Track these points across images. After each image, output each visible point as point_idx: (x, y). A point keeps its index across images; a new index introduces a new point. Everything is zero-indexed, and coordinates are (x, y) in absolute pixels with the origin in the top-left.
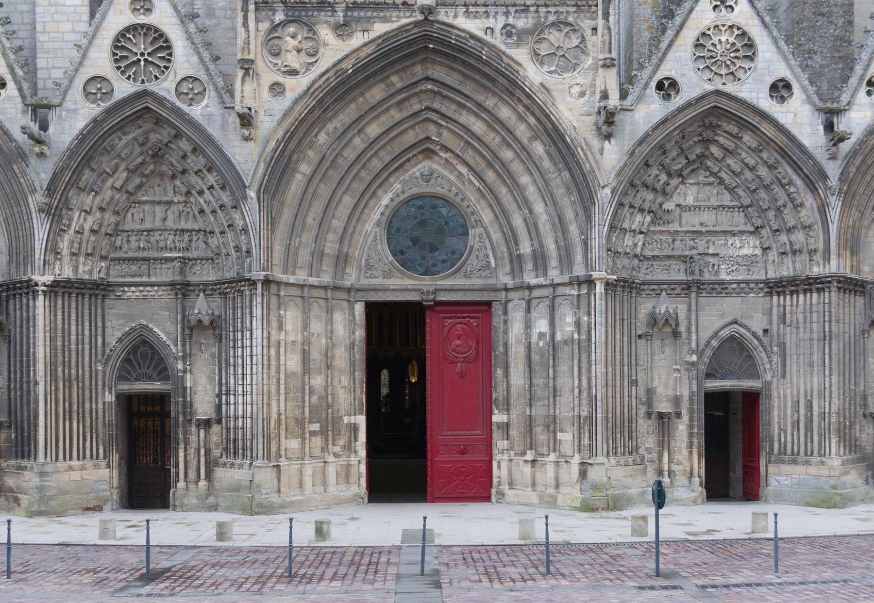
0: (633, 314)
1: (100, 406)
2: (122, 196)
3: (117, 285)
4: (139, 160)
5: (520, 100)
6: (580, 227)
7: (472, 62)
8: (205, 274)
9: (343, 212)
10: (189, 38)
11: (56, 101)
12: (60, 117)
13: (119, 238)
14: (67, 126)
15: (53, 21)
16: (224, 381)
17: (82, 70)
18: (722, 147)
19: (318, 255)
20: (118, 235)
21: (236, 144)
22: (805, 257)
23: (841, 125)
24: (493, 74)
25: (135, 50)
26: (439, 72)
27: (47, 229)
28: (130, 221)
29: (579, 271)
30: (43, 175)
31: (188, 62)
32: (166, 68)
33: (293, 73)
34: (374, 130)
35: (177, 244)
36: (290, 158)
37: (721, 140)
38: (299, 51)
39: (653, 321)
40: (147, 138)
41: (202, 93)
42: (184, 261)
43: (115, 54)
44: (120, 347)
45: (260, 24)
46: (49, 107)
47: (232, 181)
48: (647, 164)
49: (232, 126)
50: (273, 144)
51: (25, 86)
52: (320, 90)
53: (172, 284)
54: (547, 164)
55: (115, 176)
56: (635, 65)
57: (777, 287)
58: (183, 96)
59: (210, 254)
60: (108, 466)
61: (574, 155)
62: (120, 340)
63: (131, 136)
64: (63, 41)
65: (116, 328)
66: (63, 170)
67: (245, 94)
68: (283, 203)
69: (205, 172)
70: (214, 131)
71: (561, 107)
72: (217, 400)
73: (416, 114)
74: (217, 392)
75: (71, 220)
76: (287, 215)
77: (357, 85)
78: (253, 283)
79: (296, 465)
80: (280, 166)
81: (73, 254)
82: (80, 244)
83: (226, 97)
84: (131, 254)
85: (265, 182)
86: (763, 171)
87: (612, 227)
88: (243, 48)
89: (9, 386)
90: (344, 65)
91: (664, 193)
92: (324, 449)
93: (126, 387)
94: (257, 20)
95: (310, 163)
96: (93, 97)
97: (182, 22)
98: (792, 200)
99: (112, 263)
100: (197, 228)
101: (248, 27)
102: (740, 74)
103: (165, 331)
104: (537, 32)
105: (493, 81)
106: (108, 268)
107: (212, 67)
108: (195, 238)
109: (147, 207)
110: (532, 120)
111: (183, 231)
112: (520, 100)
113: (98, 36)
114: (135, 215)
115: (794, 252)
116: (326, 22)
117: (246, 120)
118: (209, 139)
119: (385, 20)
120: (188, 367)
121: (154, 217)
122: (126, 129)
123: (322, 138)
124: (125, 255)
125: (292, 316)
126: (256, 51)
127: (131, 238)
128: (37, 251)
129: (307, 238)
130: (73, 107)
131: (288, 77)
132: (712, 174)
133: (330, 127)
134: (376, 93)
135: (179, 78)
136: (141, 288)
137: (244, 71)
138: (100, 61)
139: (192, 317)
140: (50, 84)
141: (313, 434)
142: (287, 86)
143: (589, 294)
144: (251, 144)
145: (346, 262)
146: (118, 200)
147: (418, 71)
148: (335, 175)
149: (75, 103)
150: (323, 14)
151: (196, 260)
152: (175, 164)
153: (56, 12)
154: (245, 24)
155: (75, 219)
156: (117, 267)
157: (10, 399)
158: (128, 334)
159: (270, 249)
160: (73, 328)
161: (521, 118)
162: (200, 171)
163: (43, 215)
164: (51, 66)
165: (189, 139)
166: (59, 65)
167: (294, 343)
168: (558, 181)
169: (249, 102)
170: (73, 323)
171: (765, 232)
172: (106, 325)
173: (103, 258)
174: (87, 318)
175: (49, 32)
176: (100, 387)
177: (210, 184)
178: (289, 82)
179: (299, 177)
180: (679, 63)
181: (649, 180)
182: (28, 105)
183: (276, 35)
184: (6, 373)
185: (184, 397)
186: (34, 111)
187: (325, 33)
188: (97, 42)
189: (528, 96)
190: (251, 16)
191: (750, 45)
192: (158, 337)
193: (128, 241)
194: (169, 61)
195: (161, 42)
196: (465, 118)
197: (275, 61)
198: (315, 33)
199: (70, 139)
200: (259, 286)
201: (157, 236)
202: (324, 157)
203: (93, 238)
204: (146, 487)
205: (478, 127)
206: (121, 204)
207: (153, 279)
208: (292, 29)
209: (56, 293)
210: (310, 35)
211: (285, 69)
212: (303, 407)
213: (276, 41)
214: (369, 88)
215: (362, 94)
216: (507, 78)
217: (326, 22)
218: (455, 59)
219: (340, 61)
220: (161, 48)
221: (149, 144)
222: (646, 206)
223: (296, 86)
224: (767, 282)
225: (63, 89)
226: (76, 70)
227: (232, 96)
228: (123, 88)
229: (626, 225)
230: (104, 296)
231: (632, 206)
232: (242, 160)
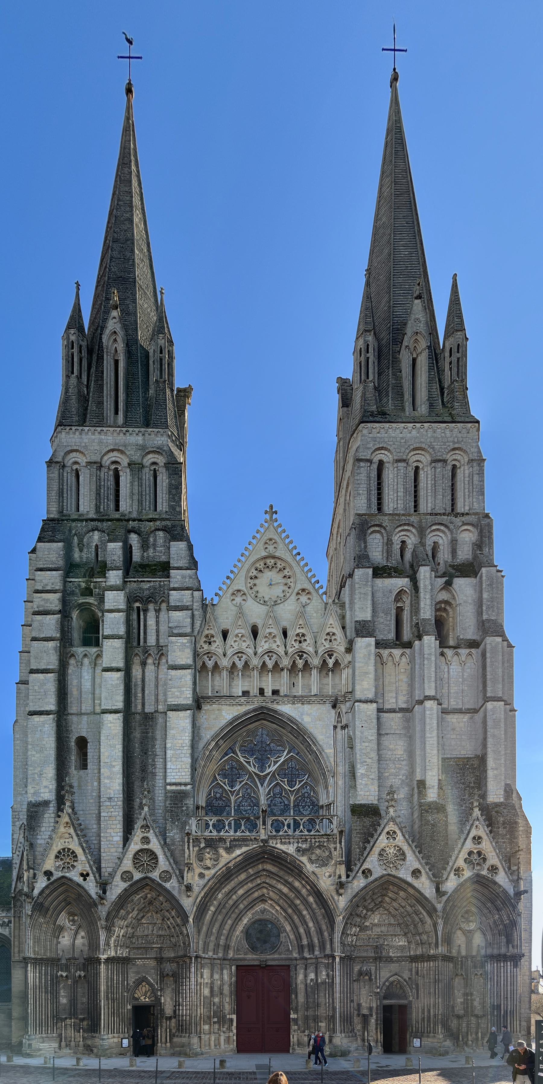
0: (352, 970)
5: (303, 879)
6: (329, 933)
7: (283, 862)
10: (165, 854)
18: (390, 898)
19: (217, 945)
22: (427, 946)
23: (443, 888)
24: (292, 868)
26: (269, 867)
29: (328, 951)
33: (208, 868)
34: (241, 892)
37: (390, 895)
38: (211, 859)
39: (360, 973)
41: (170, 878)
42: (161, 948)
48: (358, 906)
50: (199, 899)
51: (97, 875)
54: (314, 906)
56: (353, 863)
57: (414, 959)
61: (326, 902)
68: (203, 924)
70: (175, 893)
71: (321, 881)
73: (259, 885)
79: (207, 1036)
80: (202, 909)
83: (180, 879)
86: (409, 908)
87: (343, 933)
90: (229, 865)
91: (365, 918)
94: (193, 847)
95: (214, 906)
98: (422, 921)
102: (399, 867)
104: (310, 850)
105: (292, 871)
107: (174, 866)
110: (308, 887)
112: (303, 879)
115: (422, 944)
117: (189, 888)
118: (173, 896)
119: (247, 845)
123: (220, 896)
126: (193, 860)
132: (387, 910)
133: (223, 891)
134: (243, 876)
140: (106, 874)
143: (333, 962)
144: (191, 899)
145: (228, 948)
147: (260, 867)
148: (224, 911)
154: (189, 848)
159: (198, 943)
161: (304, 886)
164: (107, 867)
165: (164, 897)
168: (319, 913)
169: (190, 881)
171: (410, 935)
178: (206, 872)
179: (210, 912)
180: (372, 862)
181: (359, 913)
187: (222, 852)
189: (307, 877)
190: (191, 844)
195: (153, 856)
196: (280, 886)
205: (285, 890)
215: (237, 877)
216: (298, 869)
218: (276, 861)
219: (228, 863)
222: (357, 924)
223: (209, 874)
224: (410, 957)
227: (183, 879)
229: (349, 932)
231: (351, 924)
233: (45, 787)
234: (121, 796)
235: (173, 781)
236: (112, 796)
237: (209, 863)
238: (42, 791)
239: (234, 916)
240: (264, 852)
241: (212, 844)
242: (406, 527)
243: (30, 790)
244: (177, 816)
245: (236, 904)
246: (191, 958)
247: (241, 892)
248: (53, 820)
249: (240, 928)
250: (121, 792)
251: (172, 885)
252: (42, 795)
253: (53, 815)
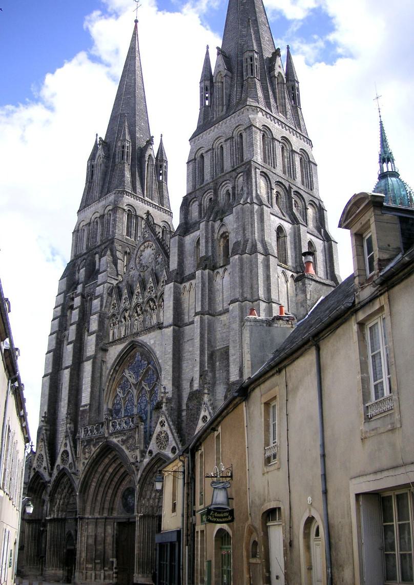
9: (109, 495)
33: (86, 459)
34: (111, 470)
36: (87, 483)
38: (88, 452)
50: (81, 479)
53: (74, 518)
60: (63, 570)
65: (67, 530)
68: (88, 495)
75: (57, 502)
76: (90, 497)
77: (98, 461)
82: (59, 508)
92: (101, 569)
106: (66, 514)
125: (91, 528)
129: (98, 504)
134: (107, 461)
141: (98, 563)
167: (92, 536)
179: (93, 487)
191: (168, 437)
202: (98, 480)
214: (104, 459)
223: (86, 462)
239: (112, 487)
240: (108, 445)
241: (89, 441)
242: (209, 191)
245: (111, 479)
247: (111, 470)
249: (119, 494)
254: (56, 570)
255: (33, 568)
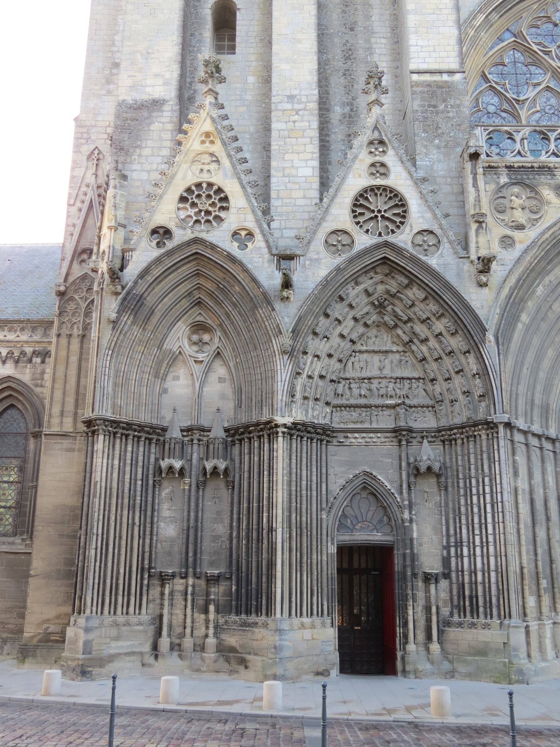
1: (325, 558)
2: (346, 344)
3: (340, 431)
4: (365, 310)
8: (426, 421)
10: (422, 196)
11: (298, 252)
12: (304, 266)
13: (341, 385)
14: (310, 273)
15: (286, 189)
16: (452, 532)
17: (324, 224)
20: (339, 382)
21: (471, 290)
25: (372, 208)
27: (290, 371)
28: (351, 369)
30: (287, 320)
31: (422, 217)
32: (403, 223)
33: (520, 227)
35: (398, 391)
40: (376, 289)
43: (354, 211)
44: (342, 494)
45: (487, 186)
46: (290, 258)
47: (467, 326)
49: (467, 275)
52: (548, 242)
53: (396, 431)
55: (343, 325)
58: (417, 248)
59: (431, 403)
62: (343, 488)
63: (362, 287)
64: (296, 206)
66: (306, 314)
67: (480, 245)
69: (433, 319)
70: (451, 277)
72: (445, 552)
74: (445, 544)
78: (491, 426)
81: (305, 398)
84: (352, 401)
85: (502, 326)
88: (475, 205)
89: (231, 534)
93: (346, 538)
96: (334, 248)
97: (416, 183)
99: (334, 410)
100: (417, 377)
101: (478, 187)
103: (387, 479)
108: (414, 386)
109: (365, 356)
111: (403, 378)
113: (339, 195)
114: (355, 363)
116: (547, 184)
118: (447, 286)
120: (414, 517)
121: (373, 366)
122: (360, 279)
123: (540, 291)
124: (348, 402)
127: (352, 386)
128: (280, 393)
130: (316, 257)
131: (516, 231)
135: (415, 231)
136: (364, 435)
137: (477, 224)
138: (340, 215)
139: (421, 464)
142: (516, 239)
144: (486, 290)
146: (343, 348)
149: (318, 253)
150: (543, 177)
151: (415, 407)
152: (400, 313)
153: (289, 182)
154: (475, 185)
155: (308, 364)
156: (338, 414)
157: (231, 548)
158: (351, 481)
160: (304, 473)
162: (428, 318)
163: (286, 357)
166: (290, 226)
170: (304, 467)
172: (329, 473)
173: (328, 404)
174: (314, 463)
175: (282, 199)
176: (324, 537)
177: (439, 331)
178: (517, 235)
179: (520, 326)
182: (274, 255)
183: (500, 195)
184: (227, 521)
185: (412, 549)
186: (279, 261)
187: (547, 194)
188: (337, 200)
190: (480, 177)
192: (382, 485)
193: (350, 388)
194: (404, 217)
197: (502, 218)
198: (537, 193)
199: (313, 286)
200: (501, 428)
201: (375, 385)
203: (321, 383)
204: (370, 647)
206: (344, 353)
207: (374, 425)
208: (516, 189)
209: (291, 435)
210: (533, 195)
211: (513, 224)
212: (536, 560)
213: (502, 200)
217: (547, 184)
220: (396, 206)
221: (376, 296)
225: (306, 241)
226: (319, 224)
228: (363, 241)
230: (328, 441)
232: (478, 305)
233: (156, 75)
234: (316, 92)
235: (424, 67)
236: (295, 92)
237: (520, 217)
238: (148, 82)
243: (124, 79)
244: (437, 128)
246: (496, 426)
248: (168, 136)
250: (315, 85)
251: (442, 261)
252: (148, 89)
253: (170, 126)
254: (313, 627)
255: (127, 624)
